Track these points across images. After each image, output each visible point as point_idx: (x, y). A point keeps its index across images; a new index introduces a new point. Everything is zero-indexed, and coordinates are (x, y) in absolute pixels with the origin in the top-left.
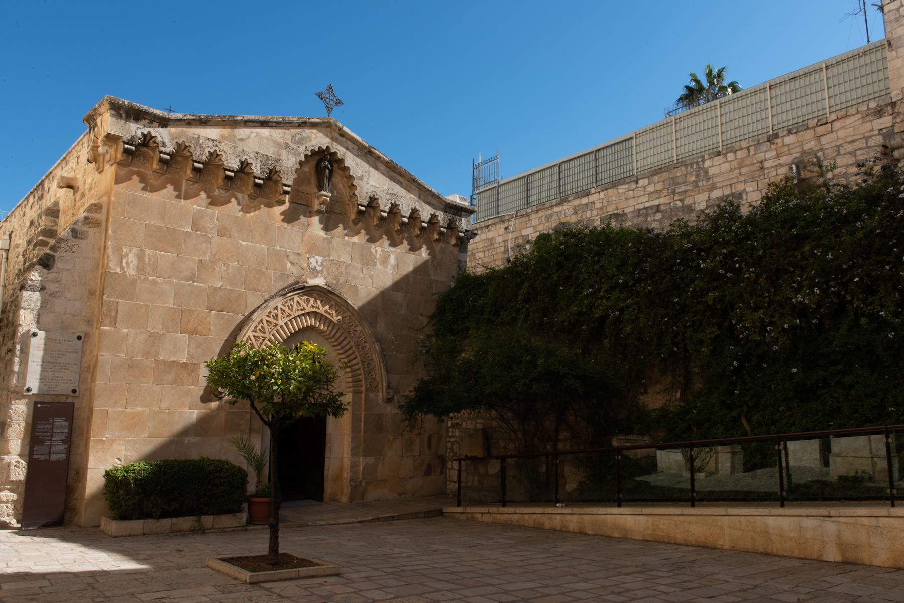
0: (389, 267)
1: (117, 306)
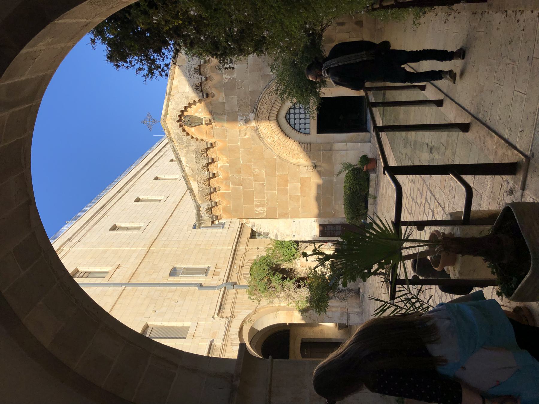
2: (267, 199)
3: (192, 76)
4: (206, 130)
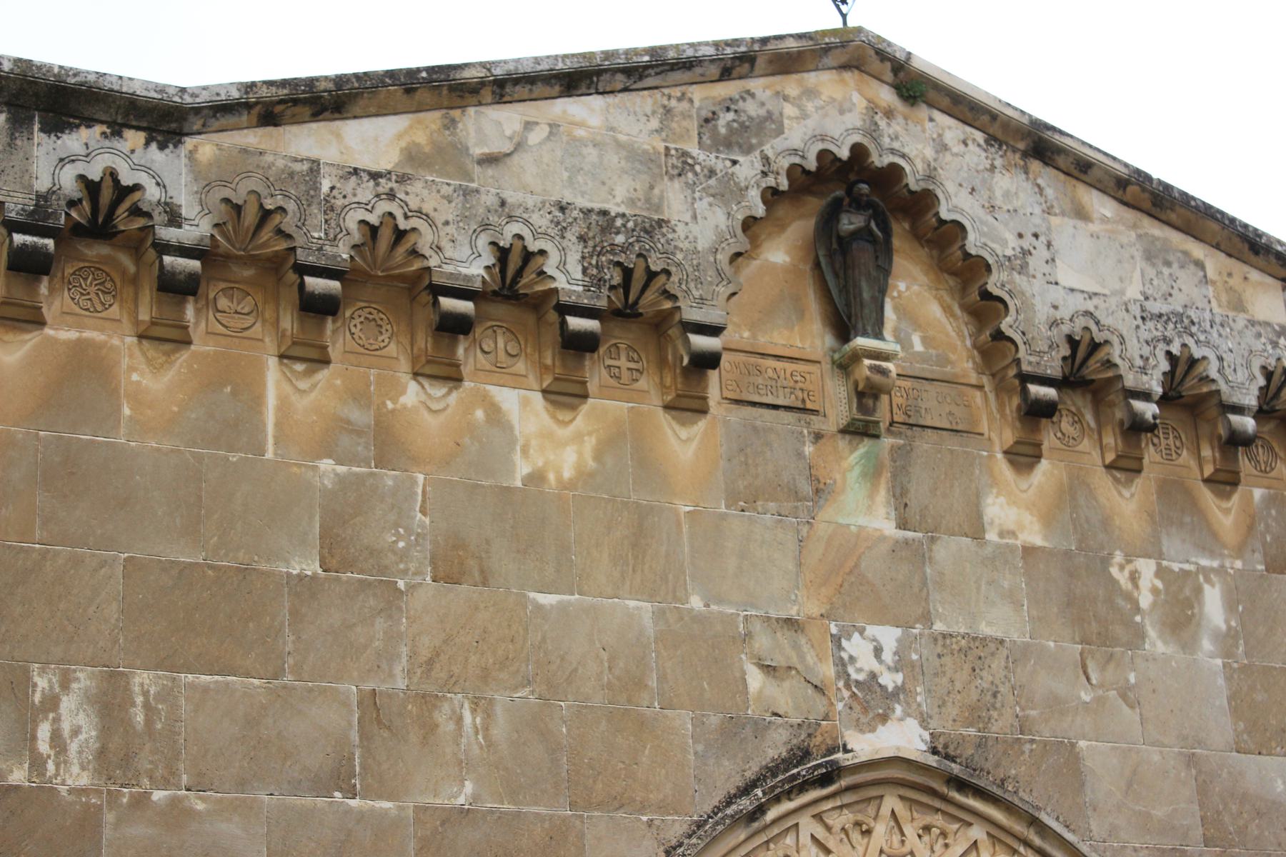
0: (1207, 644)
2: (191, 813)
3: (1151, 330)
4: (778, 357)
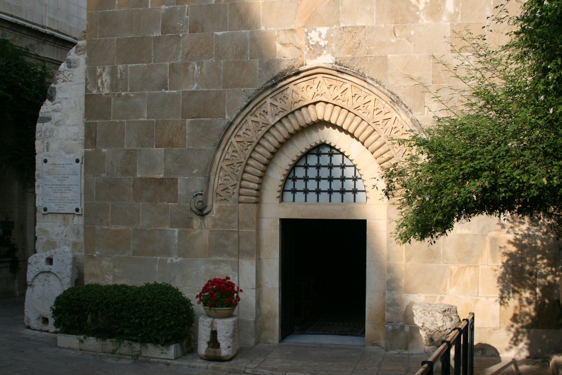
1: (96, 128)
2: (130, 97)
